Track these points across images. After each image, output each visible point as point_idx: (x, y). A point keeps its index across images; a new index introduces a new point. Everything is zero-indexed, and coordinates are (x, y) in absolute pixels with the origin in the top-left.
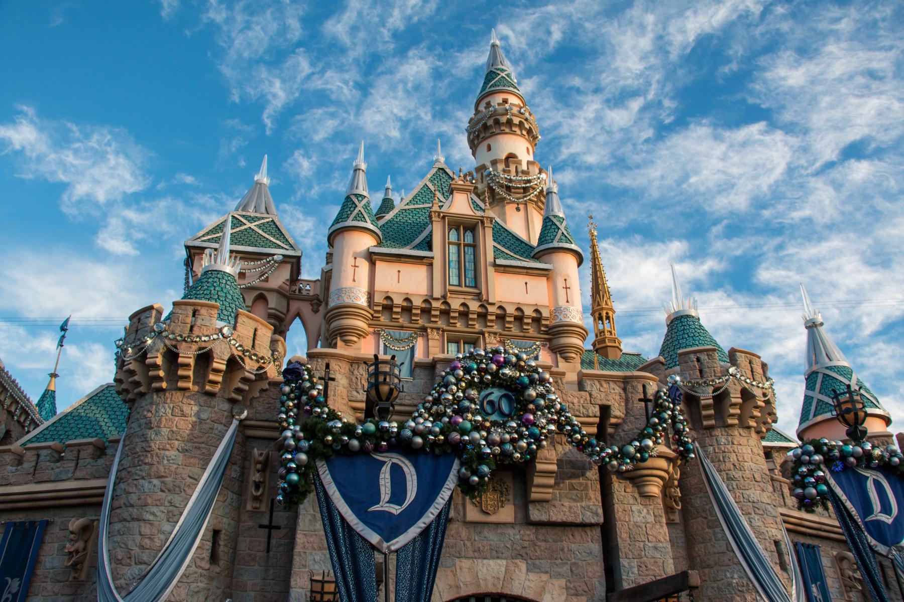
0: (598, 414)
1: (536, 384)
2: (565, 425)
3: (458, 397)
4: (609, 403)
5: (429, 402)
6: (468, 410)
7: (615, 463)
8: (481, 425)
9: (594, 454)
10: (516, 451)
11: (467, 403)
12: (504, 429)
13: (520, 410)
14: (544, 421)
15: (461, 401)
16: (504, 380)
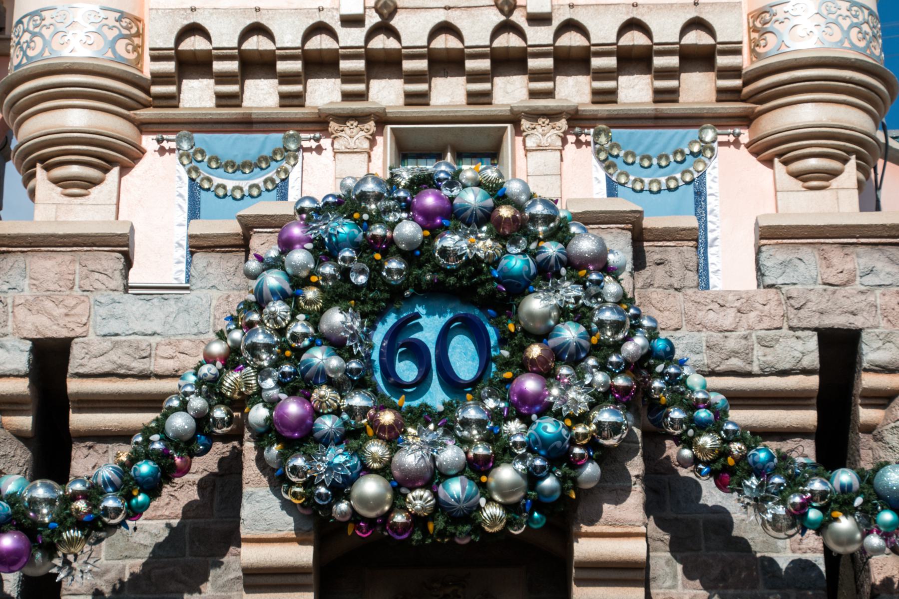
0: (812, 359)
1: (558, 275)
2: (666, 406)
3: (294, 337)
4: (857, 322)
5: (209, 359)
6: (323, 377)
7: (845, 524)
8: (374, 422)
9: (765, 500)
10: (490, 500)
11: (318, 356)
12: (449, 430)
13: (505, 364)
14: (578, 397)
15: (306, 349)
16: (450, 273)
